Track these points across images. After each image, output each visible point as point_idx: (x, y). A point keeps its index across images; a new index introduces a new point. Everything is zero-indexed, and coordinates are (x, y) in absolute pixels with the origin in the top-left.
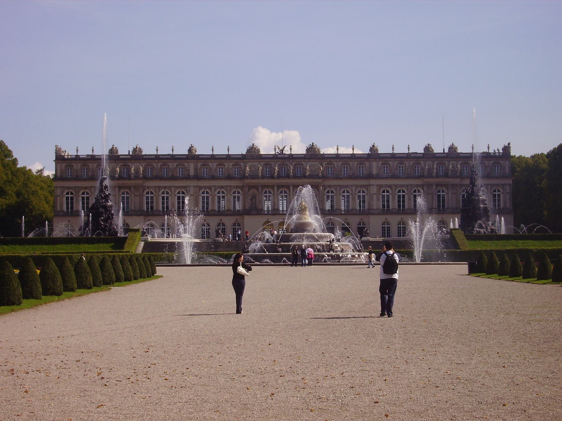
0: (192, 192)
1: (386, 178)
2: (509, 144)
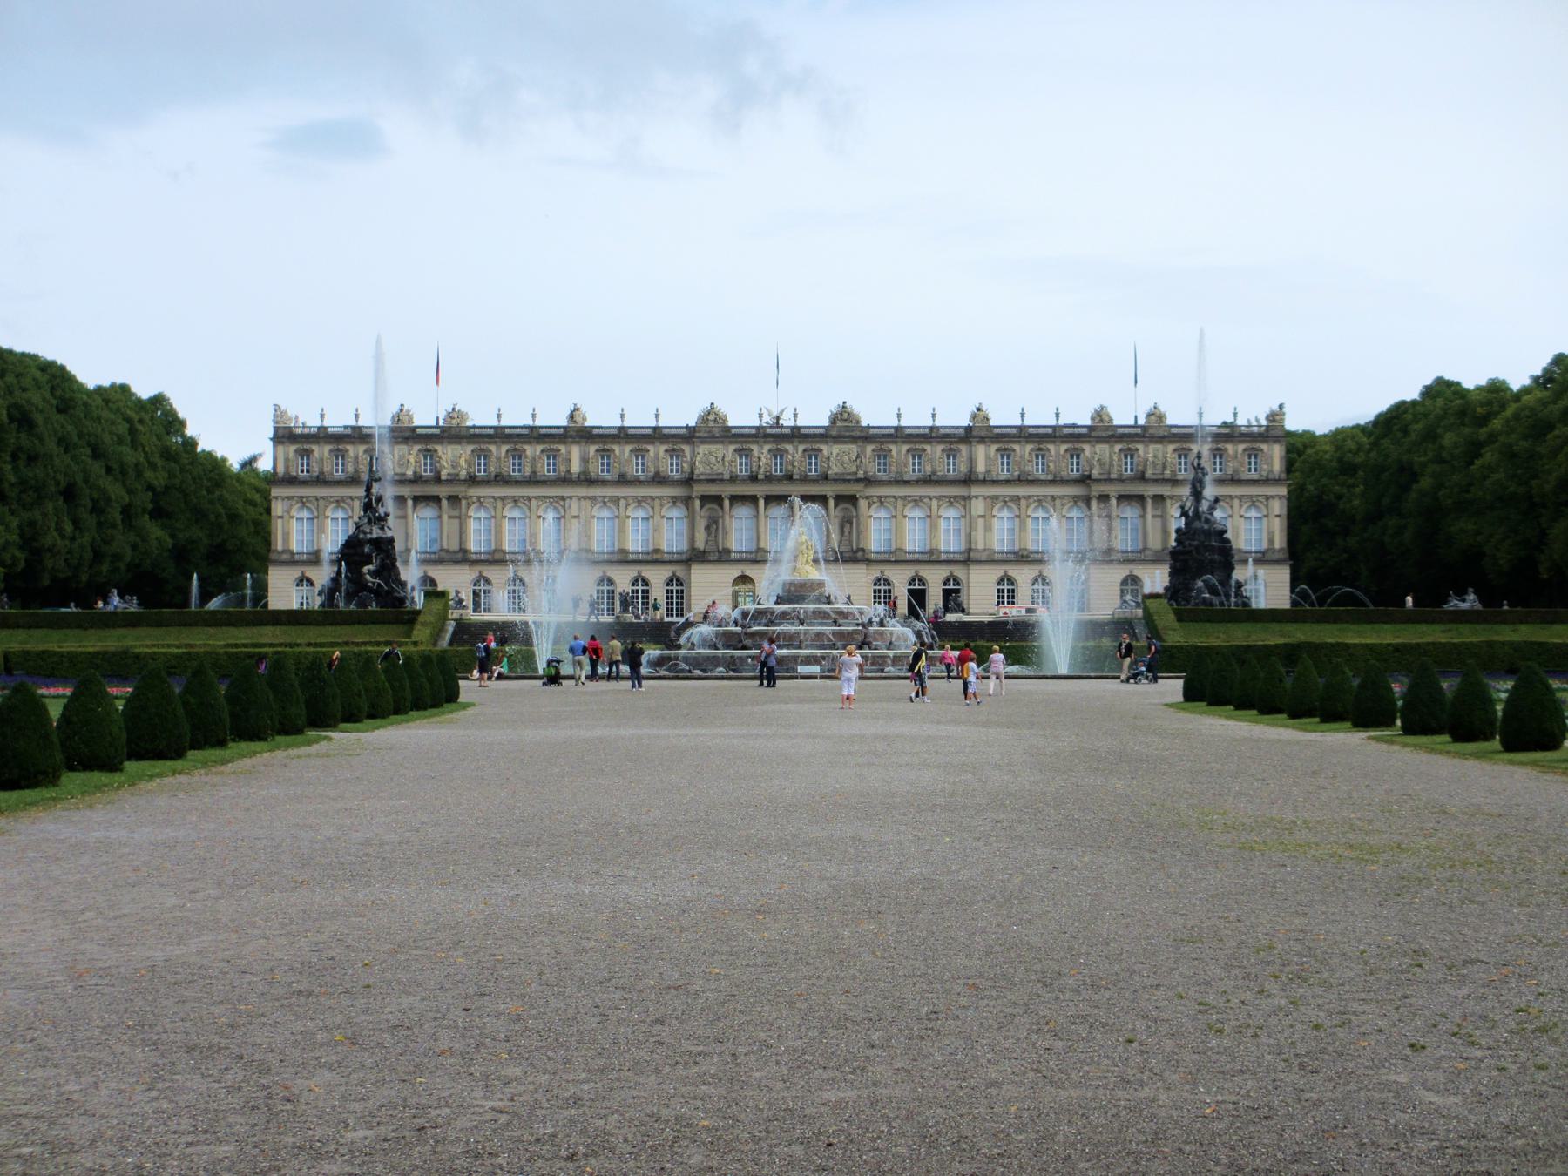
0: (574, 511)
1: (1008, 482)
2: (1281, 407)
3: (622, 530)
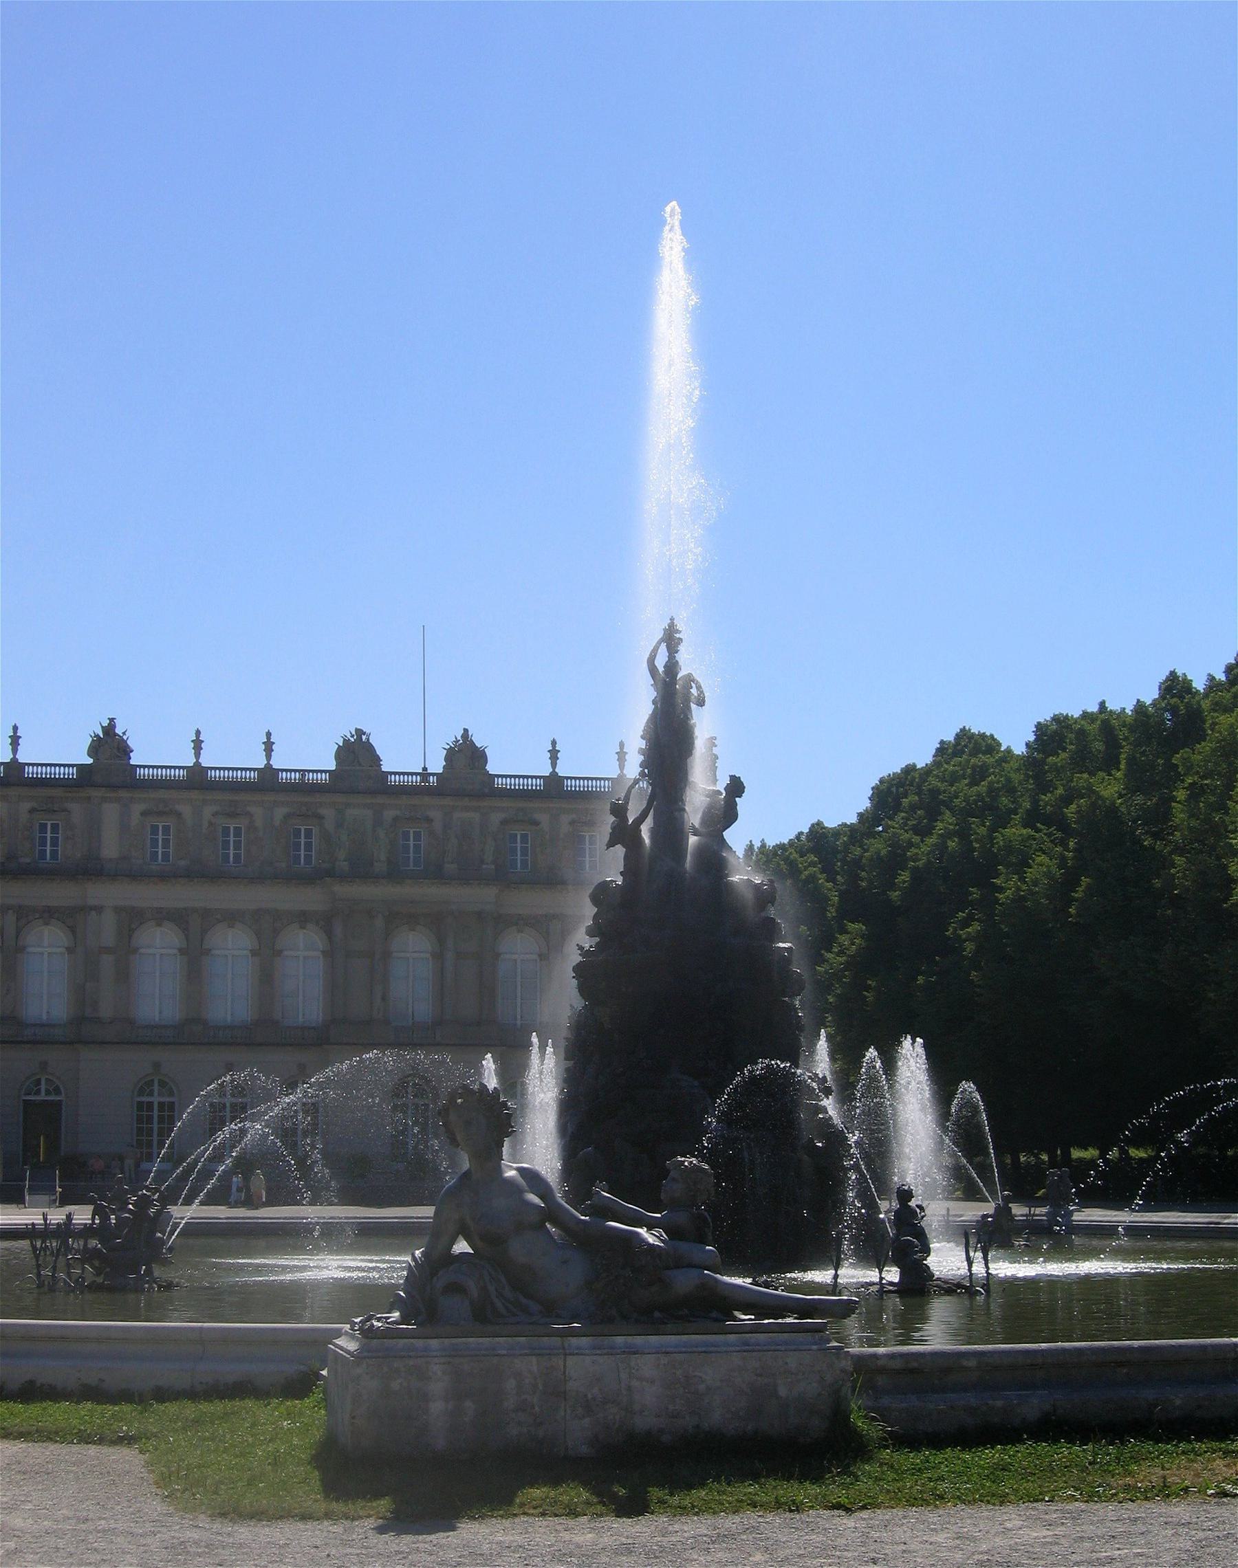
1: (164, 877)
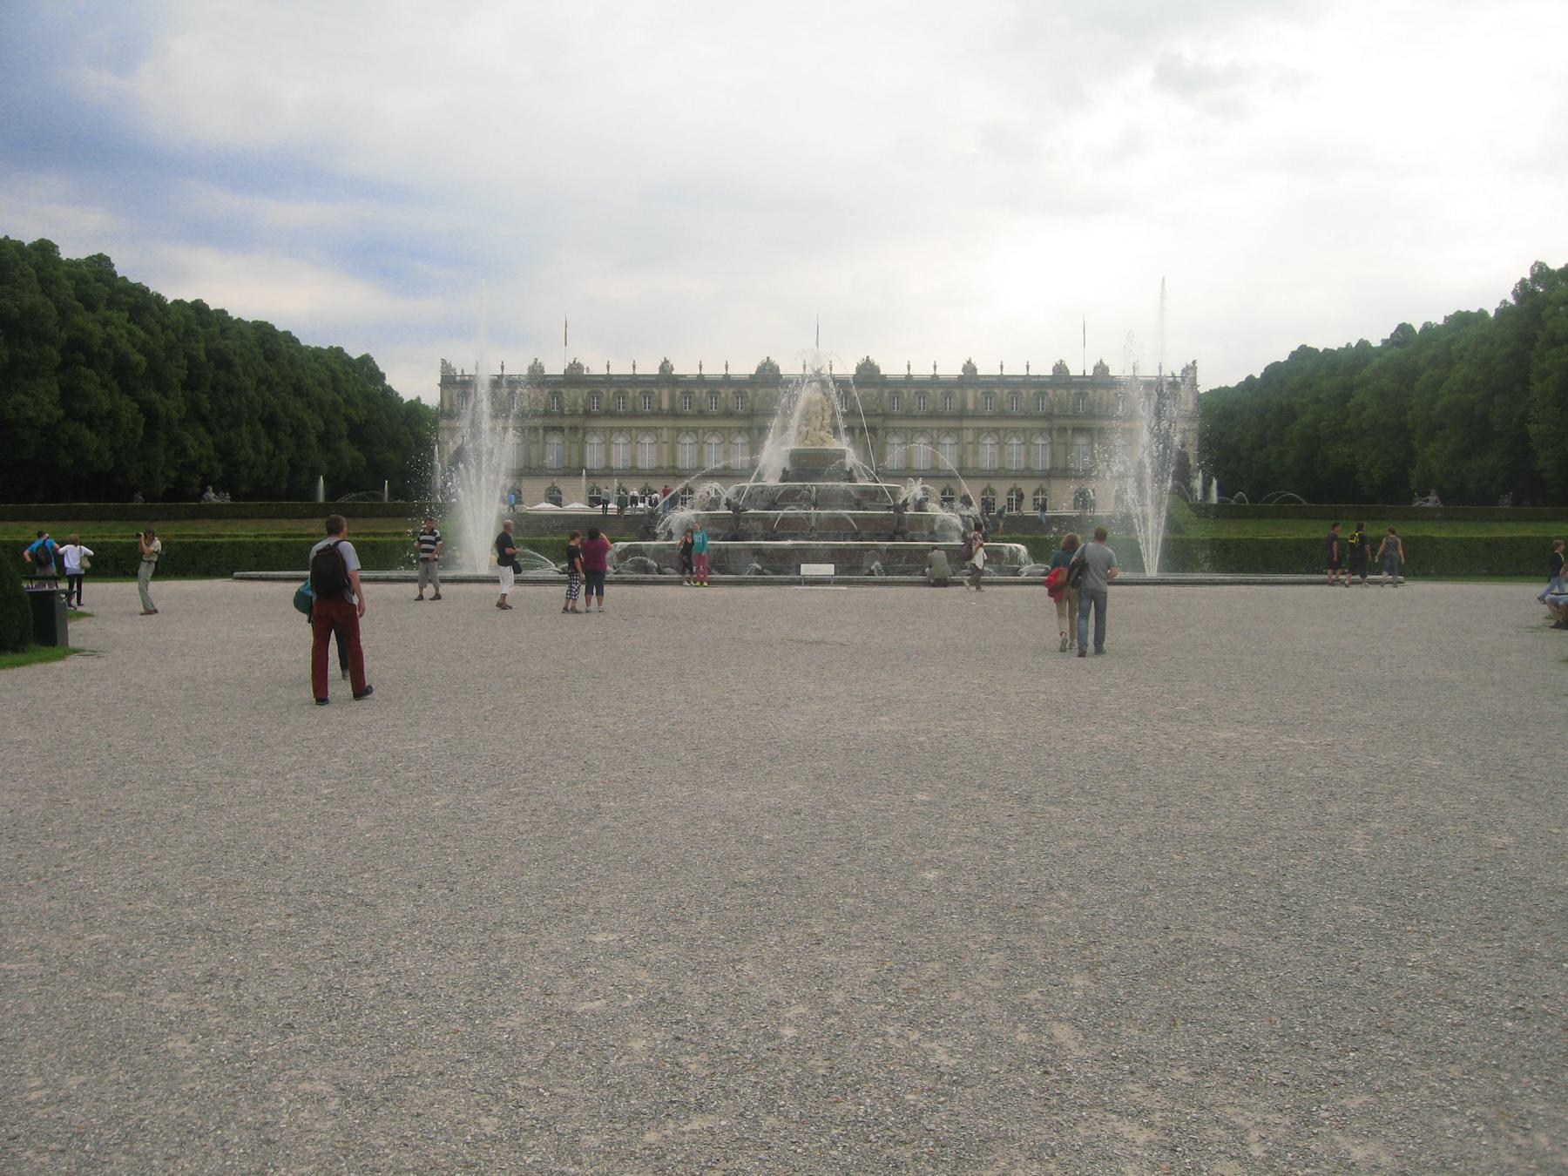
0: (665, 438)
1: (990, 417)
3: (701, 452)
